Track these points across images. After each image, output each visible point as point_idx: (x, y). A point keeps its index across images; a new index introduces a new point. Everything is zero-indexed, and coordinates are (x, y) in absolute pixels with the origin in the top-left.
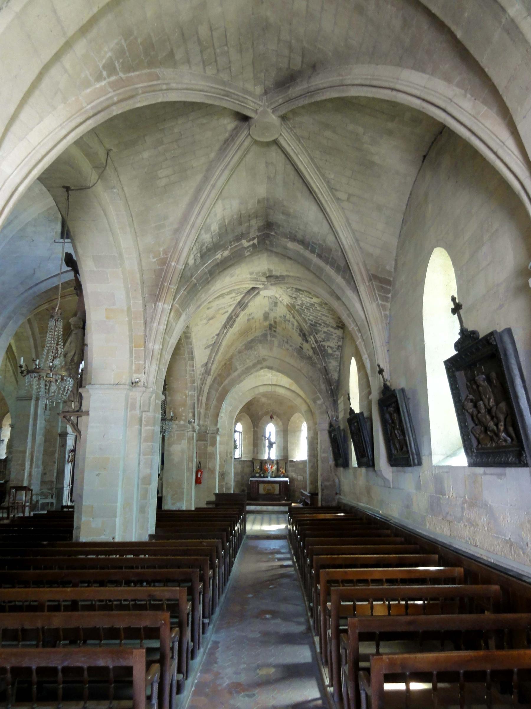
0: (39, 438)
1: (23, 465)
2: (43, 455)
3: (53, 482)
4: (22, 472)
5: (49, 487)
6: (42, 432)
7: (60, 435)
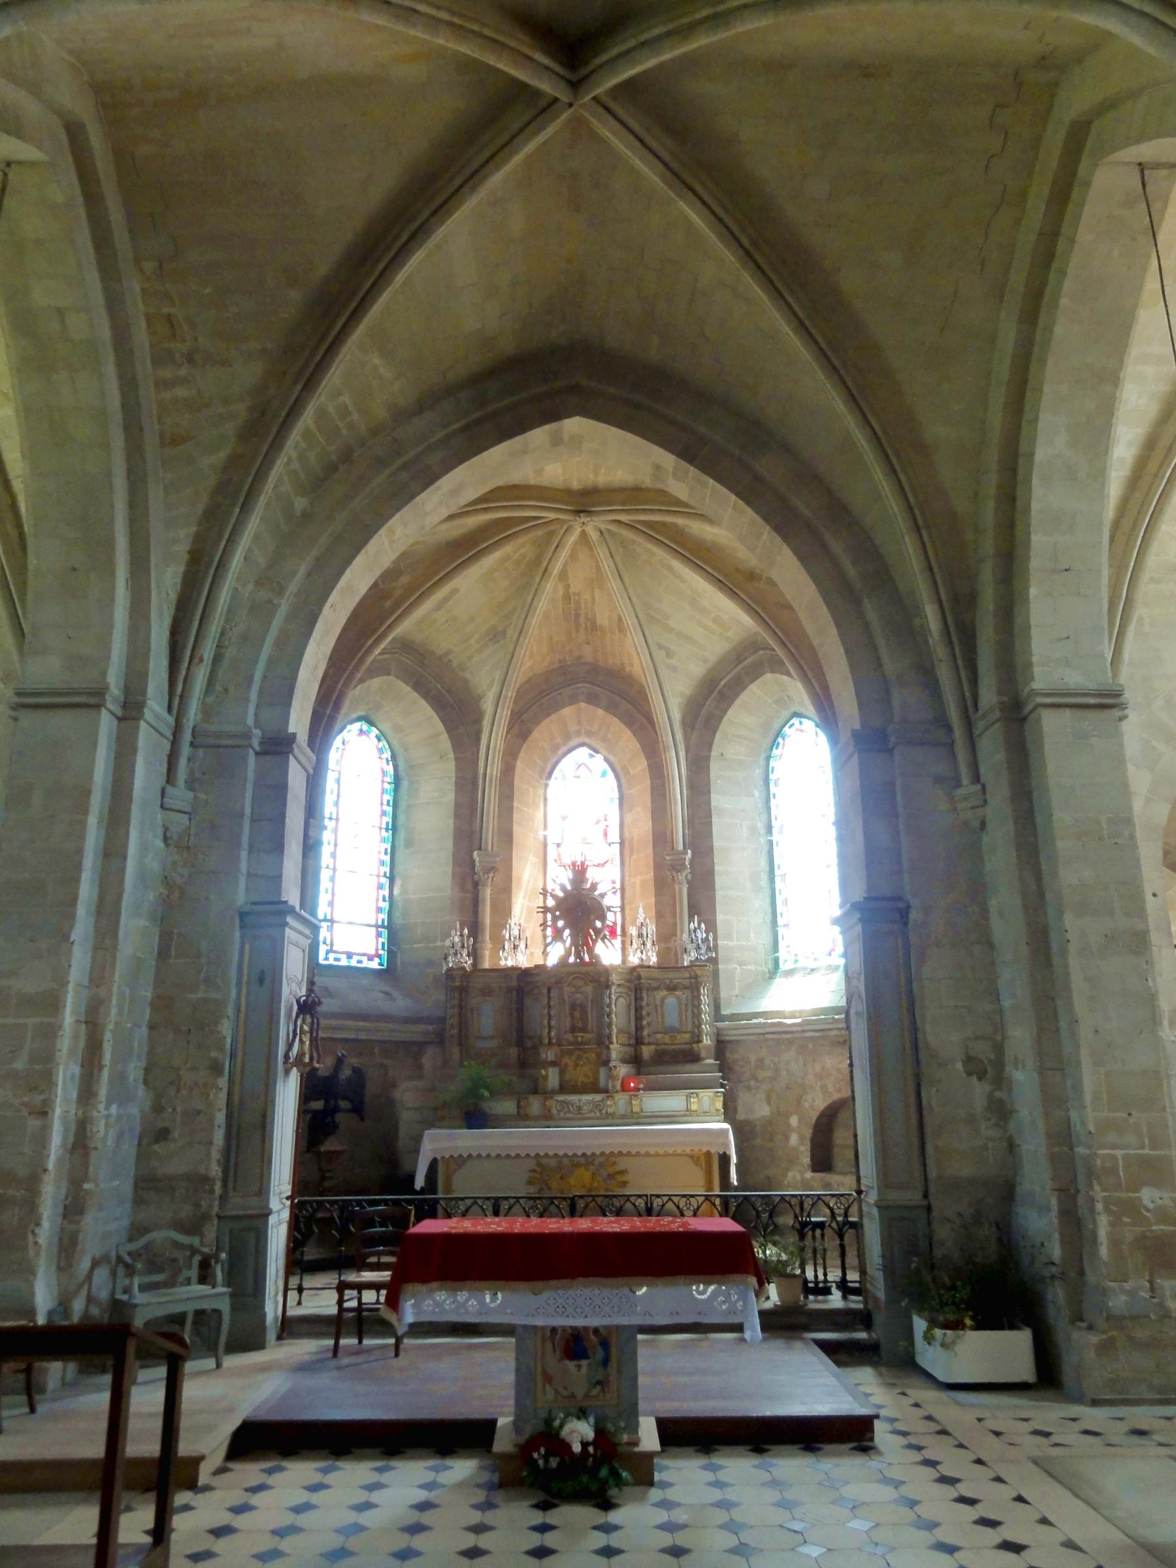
0: (135, 931)
1: (41, 1078)
2: (152, 1027)
3: (206, 1179)
4: (34, 1123)
5: (186, 1211)
6: (151, 896)
7: (242, 915)
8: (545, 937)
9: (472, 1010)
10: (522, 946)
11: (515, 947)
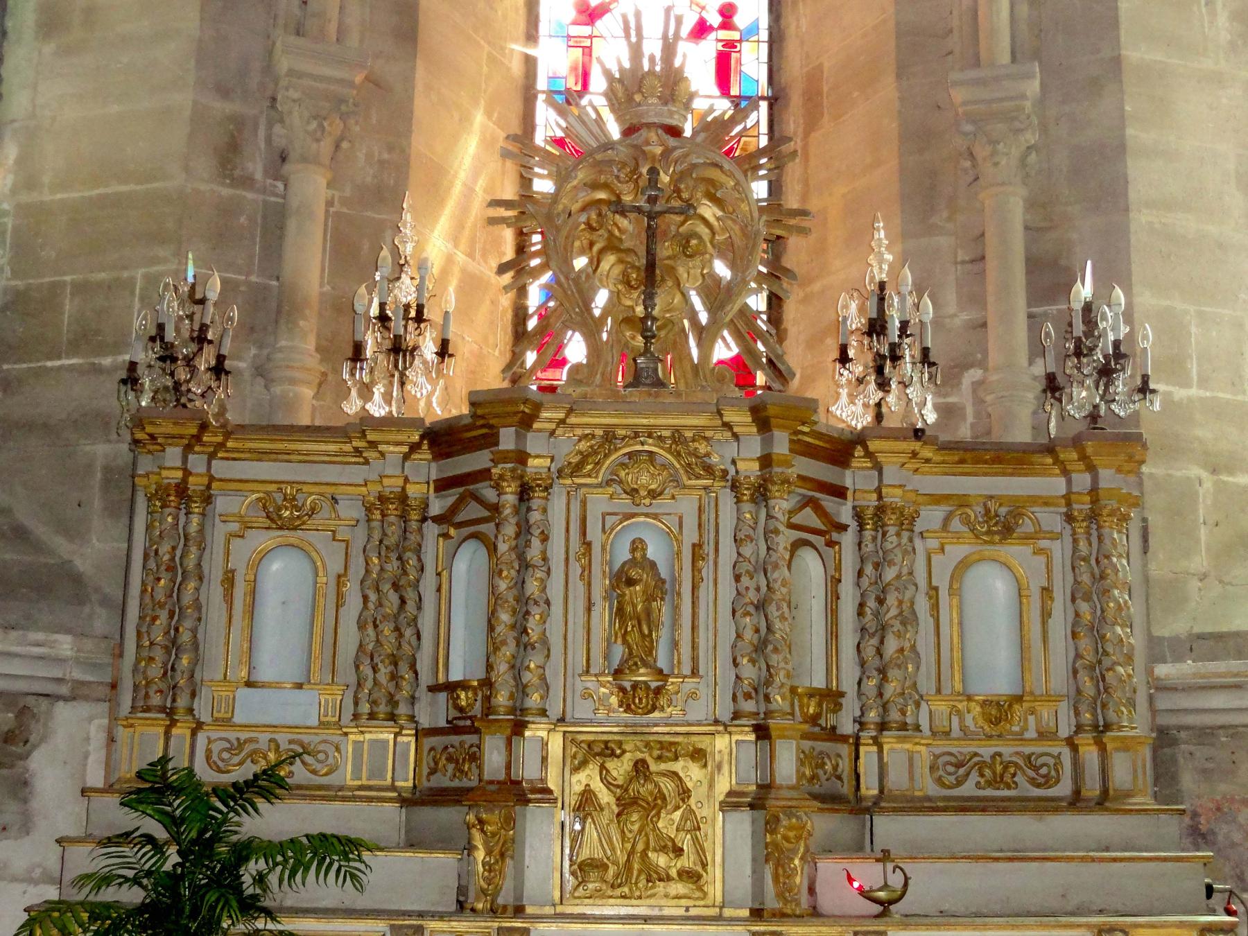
8: (520, 315)
9: (229, 580)
10: (429, 349)
11: (399, 350)
